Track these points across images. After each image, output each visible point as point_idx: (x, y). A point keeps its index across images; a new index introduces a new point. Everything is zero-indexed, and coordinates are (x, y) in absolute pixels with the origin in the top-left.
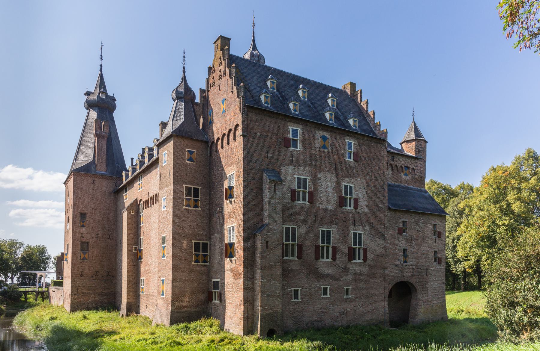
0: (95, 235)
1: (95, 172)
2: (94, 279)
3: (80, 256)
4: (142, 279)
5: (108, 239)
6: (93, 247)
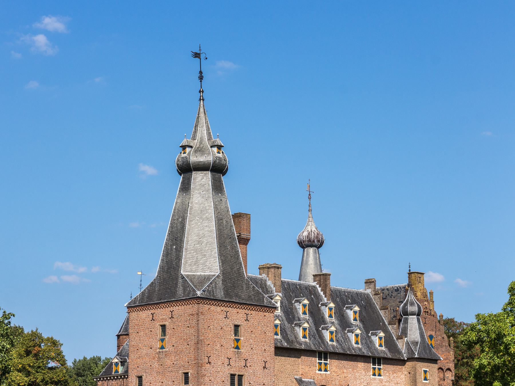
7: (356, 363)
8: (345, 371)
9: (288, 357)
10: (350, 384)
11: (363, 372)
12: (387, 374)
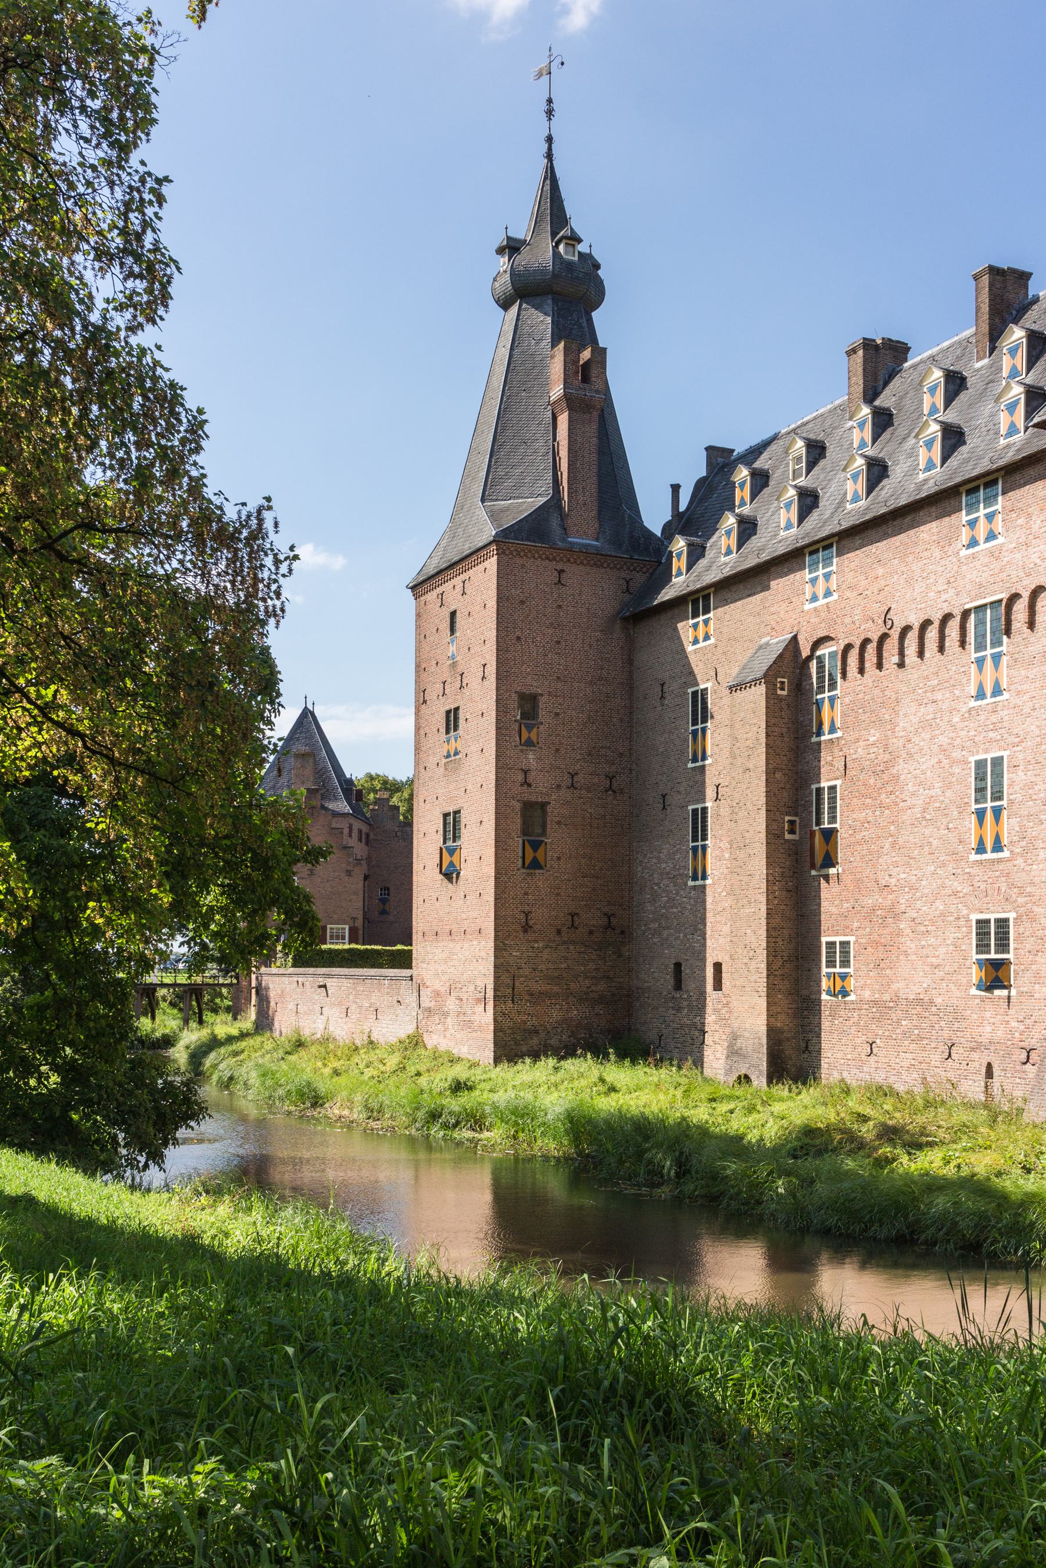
0: (567, 776)
1: (564, 540)
2: (564, 943)
3: (520, 854)
4: (831, 945)
5: (607, 791)
6: (559, 823)
7: (912, 532)
8: (880, 571)
9: (749, 596)
10: (893, 607)
11: (937, 553)
12: (1020, 521)
